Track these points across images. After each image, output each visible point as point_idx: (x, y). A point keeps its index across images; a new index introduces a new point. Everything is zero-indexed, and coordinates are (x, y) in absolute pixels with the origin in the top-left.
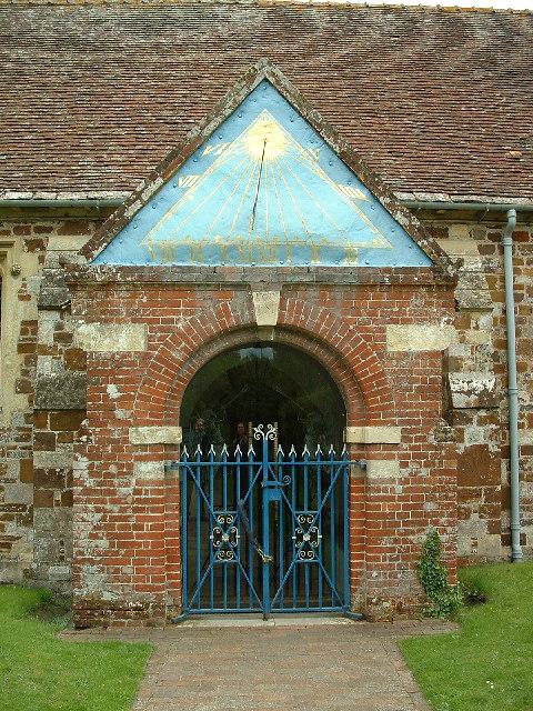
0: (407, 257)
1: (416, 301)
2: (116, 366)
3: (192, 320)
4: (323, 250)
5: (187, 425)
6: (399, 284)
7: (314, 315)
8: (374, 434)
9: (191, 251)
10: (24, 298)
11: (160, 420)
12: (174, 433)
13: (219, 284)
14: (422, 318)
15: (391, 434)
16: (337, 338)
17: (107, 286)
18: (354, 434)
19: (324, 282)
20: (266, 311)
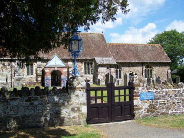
0: (64, 66)
1: (65, 68)
2: (47, 72)
3: (52, 70)
4: (59, 65)
5: (51, 75)
6: (64, 67)
7: (59, 69)
8: (62, 76)
9: (52, 65)
10: (35, 66)
11: (50, 75)
12: (51, 76)
13: (53, 67)
14: (65, 69)
15: (64, 76)
16: (60, 70)
17: (47, 68)
18: (61, 76)
19: (59, 67)
20: (56, 69)
